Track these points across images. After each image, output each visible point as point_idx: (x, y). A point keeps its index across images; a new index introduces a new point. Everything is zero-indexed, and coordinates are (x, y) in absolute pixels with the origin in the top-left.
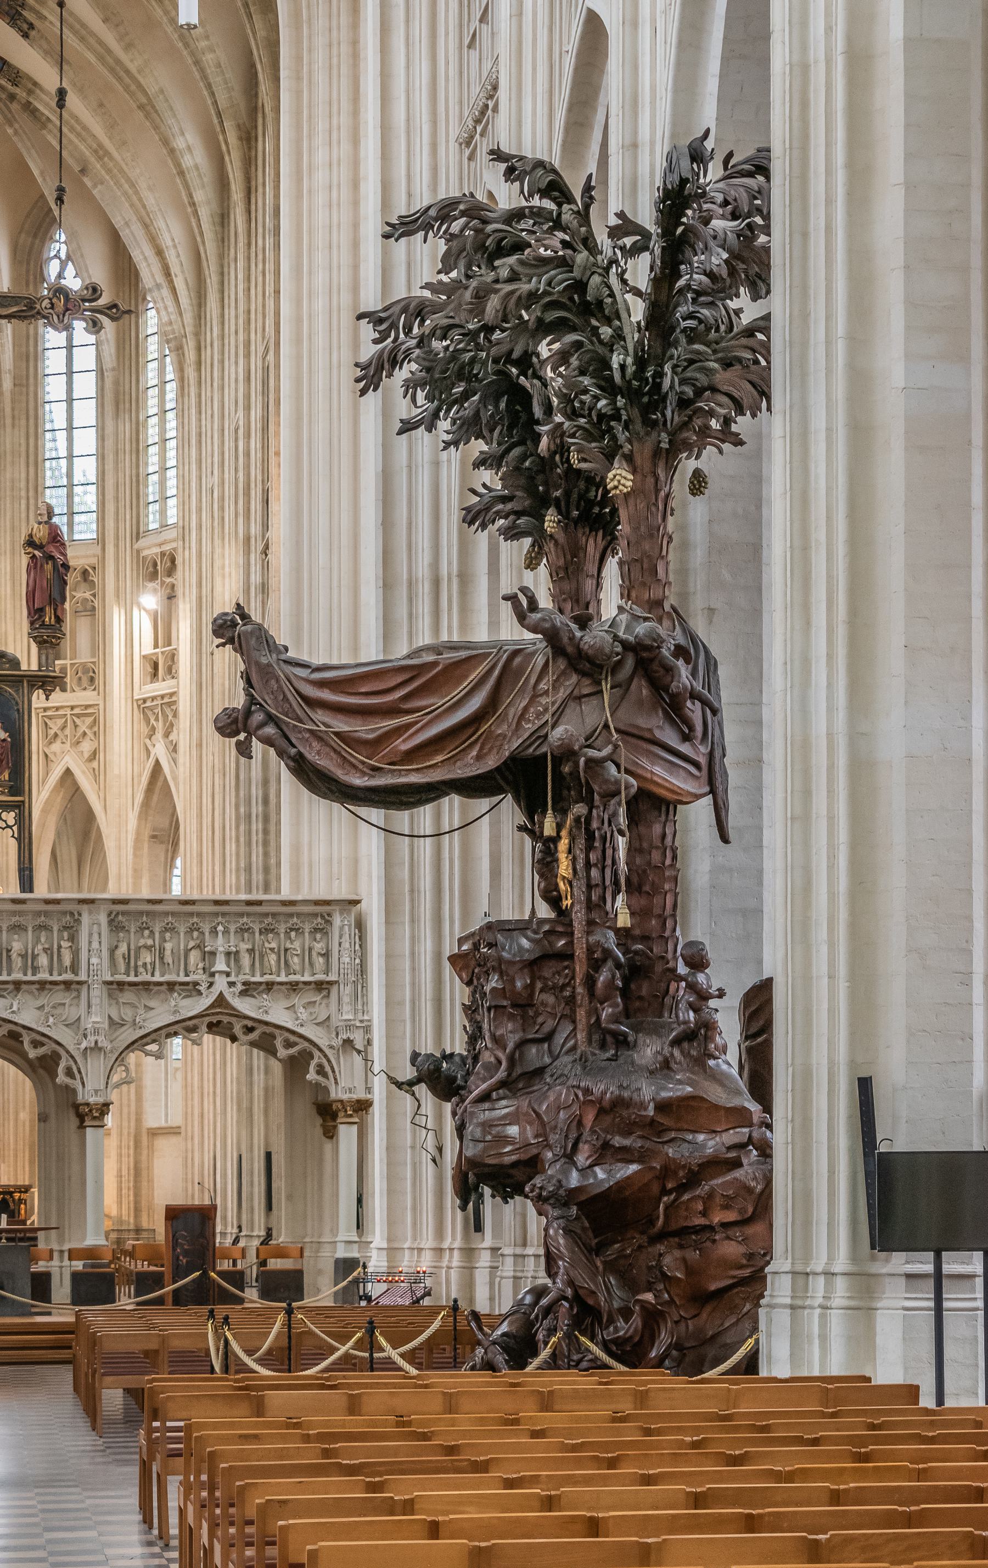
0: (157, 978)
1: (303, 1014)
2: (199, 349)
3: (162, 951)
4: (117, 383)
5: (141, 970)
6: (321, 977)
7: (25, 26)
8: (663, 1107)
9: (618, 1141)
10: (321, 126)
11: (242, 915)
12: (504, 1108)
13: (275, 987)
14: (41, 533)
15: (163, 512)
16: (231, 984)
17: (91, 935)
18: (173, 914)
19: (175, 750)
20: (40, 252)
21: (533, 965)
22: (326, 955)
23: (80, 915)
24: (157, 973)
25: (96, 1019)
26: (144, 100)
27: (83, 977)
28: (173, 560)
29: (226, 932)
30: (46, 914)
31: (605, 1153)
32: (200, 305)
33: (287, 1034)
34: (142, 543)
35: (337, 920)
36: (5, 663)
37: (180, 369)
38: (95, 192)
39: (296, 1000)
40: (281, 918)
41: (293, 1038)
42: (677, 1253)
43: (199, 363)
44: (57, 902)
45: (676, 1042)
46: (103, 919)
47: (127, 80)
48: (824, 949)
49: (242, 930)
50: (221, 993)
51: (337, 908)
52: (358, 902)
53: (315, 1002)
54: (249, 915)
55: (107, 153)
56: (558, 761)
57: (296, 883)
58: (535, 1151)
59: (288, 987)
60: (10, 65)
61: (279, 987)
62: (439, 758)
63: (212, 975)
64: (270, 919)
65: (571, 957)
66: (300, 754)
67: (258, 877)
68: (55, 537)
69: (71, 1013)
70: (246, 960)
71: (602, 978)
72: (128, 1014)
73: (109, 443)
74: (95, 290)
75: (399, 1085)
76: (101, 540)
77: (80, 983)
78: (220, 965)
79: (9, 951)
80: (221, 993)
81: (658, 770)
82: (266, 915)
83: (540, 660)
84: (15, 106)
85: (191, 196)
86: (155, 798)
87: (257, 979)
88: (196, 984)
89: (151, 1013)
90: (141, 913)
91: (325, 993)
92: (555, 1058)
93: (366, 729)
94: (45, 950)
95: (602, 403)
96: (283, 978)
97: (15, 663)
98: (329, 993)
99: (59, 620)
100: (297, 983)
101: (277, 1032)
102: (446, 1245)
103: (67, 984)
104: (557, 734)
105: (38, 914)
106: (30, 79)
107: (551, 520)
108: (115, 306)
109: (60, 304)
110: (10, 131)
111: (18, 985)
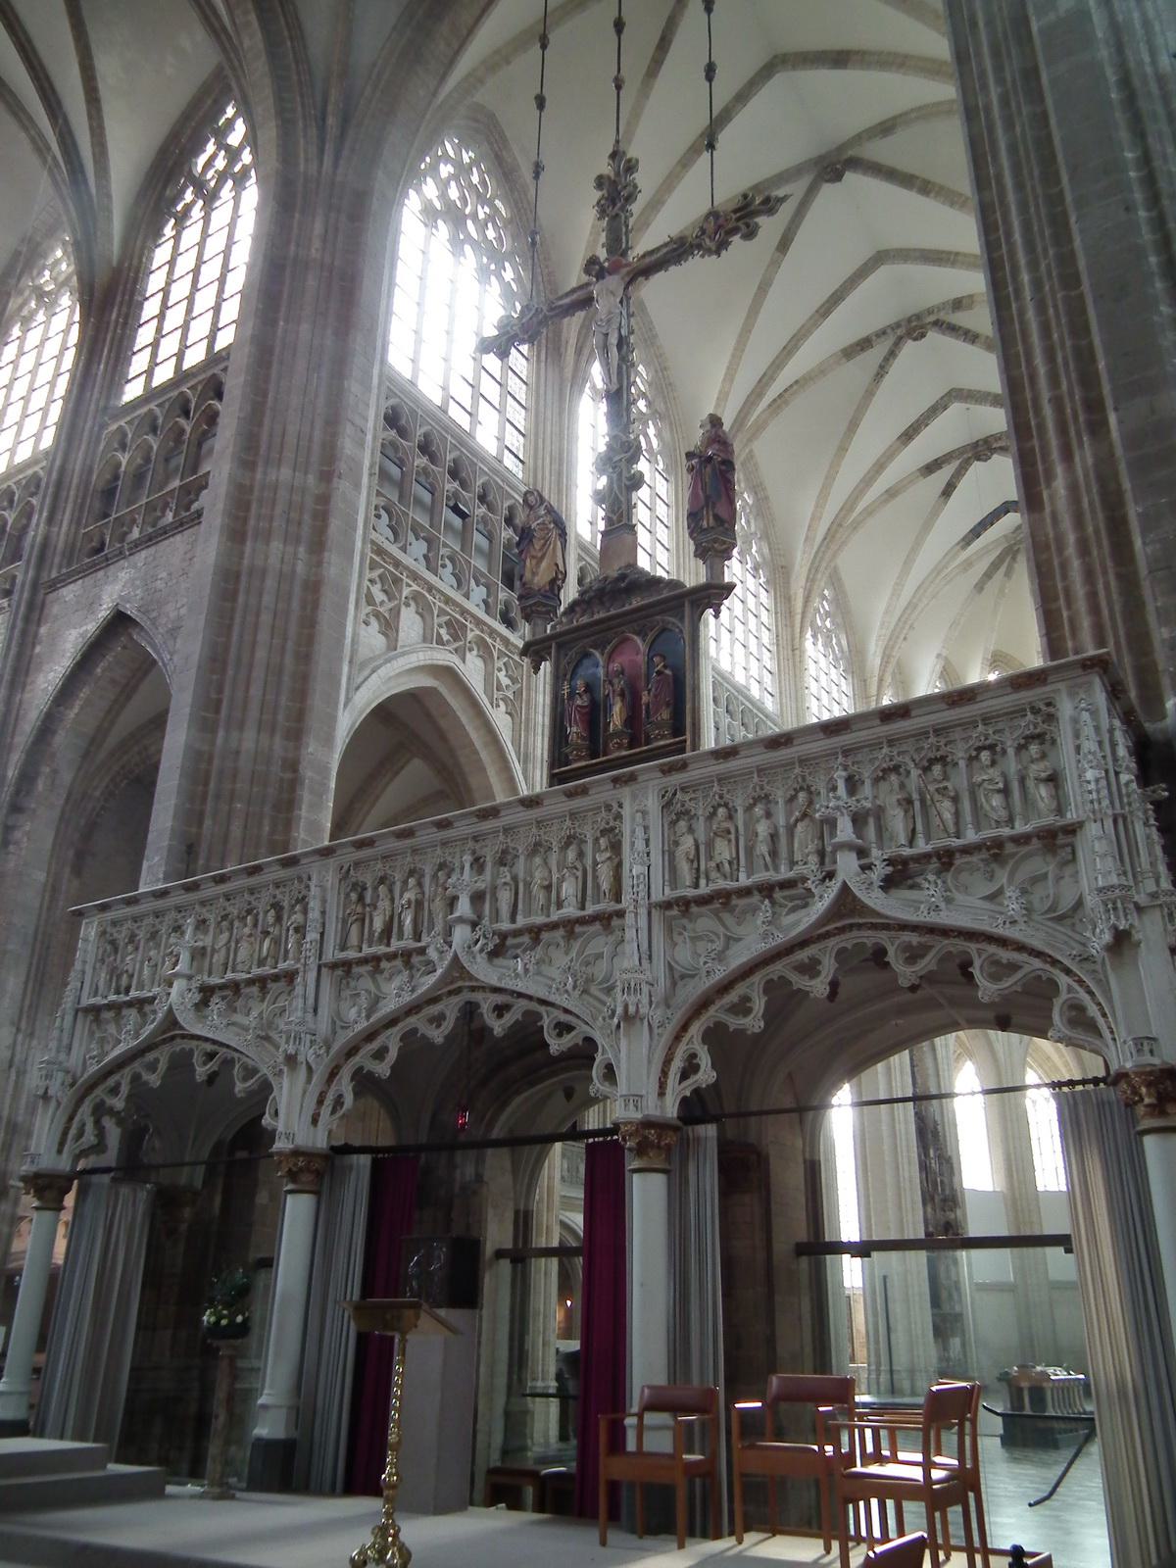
5: (714, 874)
6: (1049, 820)
13: (959, 861)
22: (1054, 779)
23: (621, 806)
24: (742, 876)
33: (992, 949)
35: (1066, 708)
36: (665, 588)
40: (957, 734)
46: (653, 803)
50: (844, 883)
51: (1061, 686)
53: (1045, 876)
59: (984, 855)
61: (967, 858)
64: (932, 739)
70: (897, 822)
79: (528, 885)
80: (844, 883)
82: (923, 734)
91: (1065, 853)
98: (1074, 853)
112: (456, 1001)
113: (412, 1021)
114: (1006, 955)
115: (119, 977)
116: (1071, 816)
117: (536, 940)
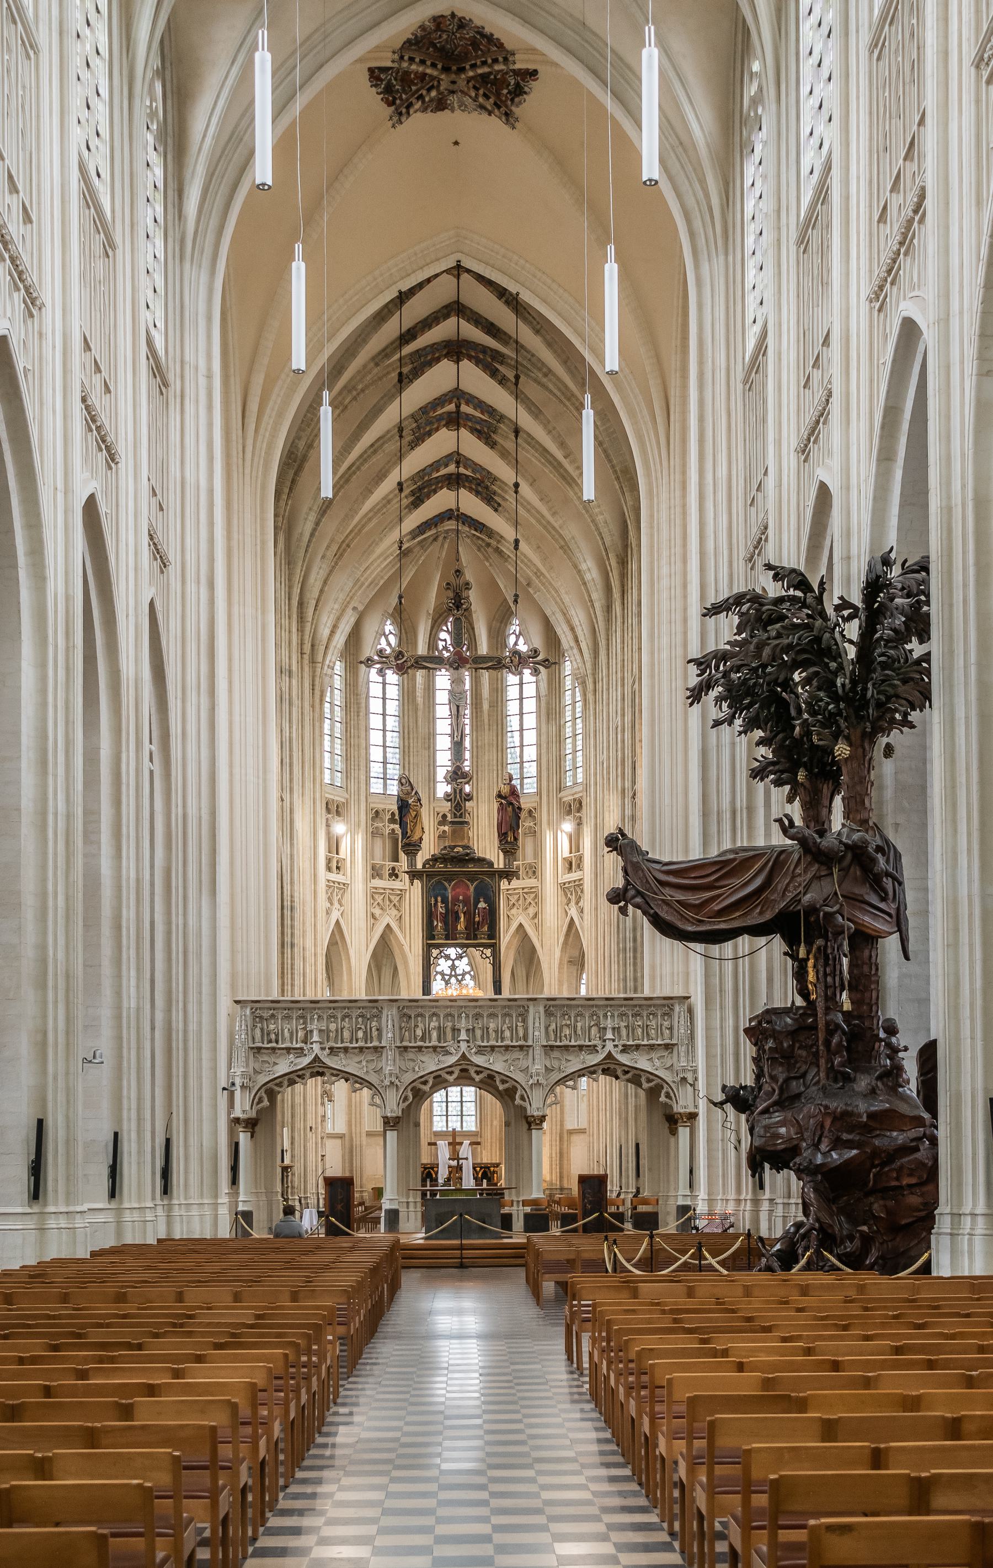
0: (573, 1043)
1: (657, 1063)
2: (595, 683)
3: (575, 1027)
4: (548, 703)
6: (668, 1041)
7: (496, 505)
8: (871, 1116)
9: (845, 1136)
10: (665, 553)
11: (621, 1006)
12: (777, 1117)
14: (505, 790)
15: (575, 776)
16: (616, 1046)
17: (534, 1019)
18: (582, 1006)
19: (582, 912)
20: (504, 631)
21: (793, 1034)
22: (671, 1029)
25: (538, 1067)
26: (563, 543)
27: (530, 1043)
28: (580, 803)
29: (612, 1016)
30: (509, 1007)
31: (837, 1144)
32: (595, 658)
34: (563, 794)
35: (677, 1008)
37: (584, 695)
38: (535, 596)
39: (654, 1055)
41: (651, 1077)
42: (881, 1202)
43: (595, 690)
44: (515, 1000)
45: (879, 1078)
46: (542, 1009)
47: (553, 533)
48: (968, 1022)
49: (622, 1015)
52: (689, 997)
54: (625, 1006)
55: (542, 574)
56: (807, 914)
57: (653, 987)
58: (796, 1143)
60: (487, 527)
62: (738, 914)
63: (605, 1041)
65: (816, 1028)
66: (656, 913)
67: (630, 984)
68: (513, 792)
69: (523, 1063)
70: (624, 1032)
71: (835, 1040)
72: (556, 1064)
73: (544, 738)
74: (536, 651)
75: (715, 1104)
76: (539, 793)
77: (528, 1046)
78: (609, 1035)
81: (867, 919)
82: (636, 1006)
83: (796, 856)
84: (490, 550)
85: (590, 596)
86: (571, 939)
87: (631, 1043)
88: (595, 1046)
89: (569, 1064)
90: (564, 1006)
92: (807, 1087)
93: (694, 898)
94: (508, 1028)
95: (831, 707)
96: (645, 1042)
97: (491, 864)
99: (516, 839)
100: (654, 1045)
101: (642, 1073)
102: (742, 1197)
103: (521, 1047)
104: (808, 897)
105: (505, 1007)
106: (498, 534)
107: (801, 776)
108: (547, 660)
109: (516, 660)
110: (487, 564)
111: (493, 1048)
112: (459, 1067)
113: (439, 1073)
114: (651, 1077)
115: (268, 1034)
116: (674, 1042)
117: (493, 1050)
